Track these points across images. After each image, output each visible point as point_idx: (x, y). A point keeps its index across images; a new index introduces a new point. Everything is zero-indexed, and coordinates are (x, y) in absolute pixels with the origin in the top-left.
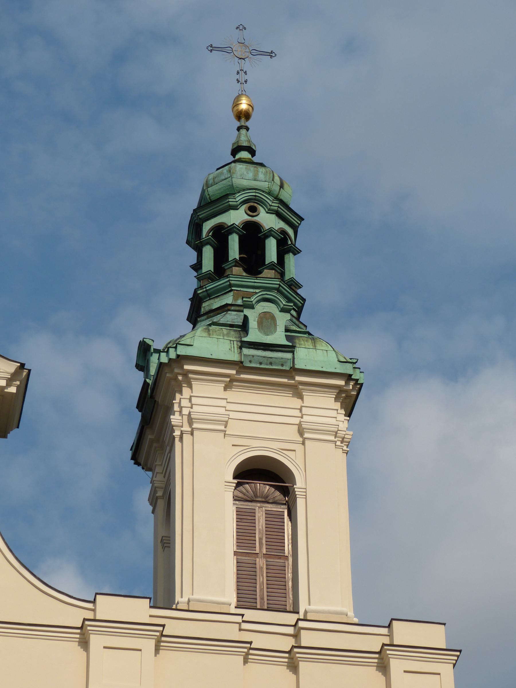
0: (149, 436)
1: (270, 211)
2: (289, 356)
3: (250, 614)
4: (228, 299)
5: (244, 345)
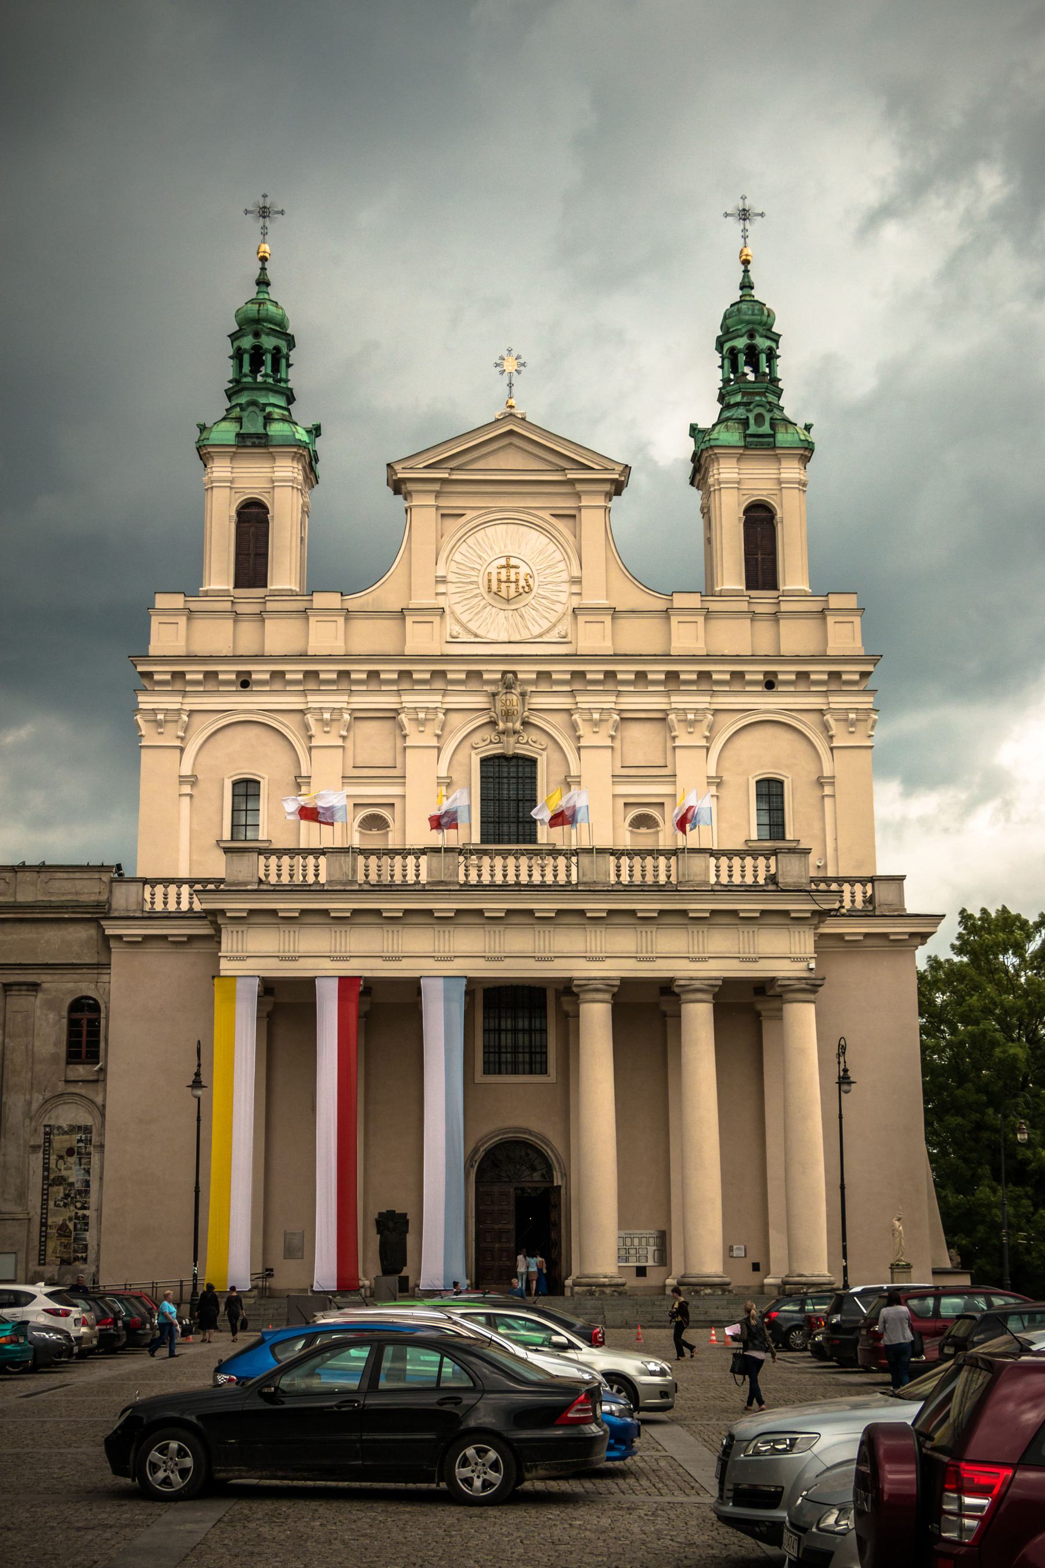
0: (698, 477)
1: (762, 336)
2: (772, 440)
3: (753, 593)
4: (738, 398)
5: (746, 436)
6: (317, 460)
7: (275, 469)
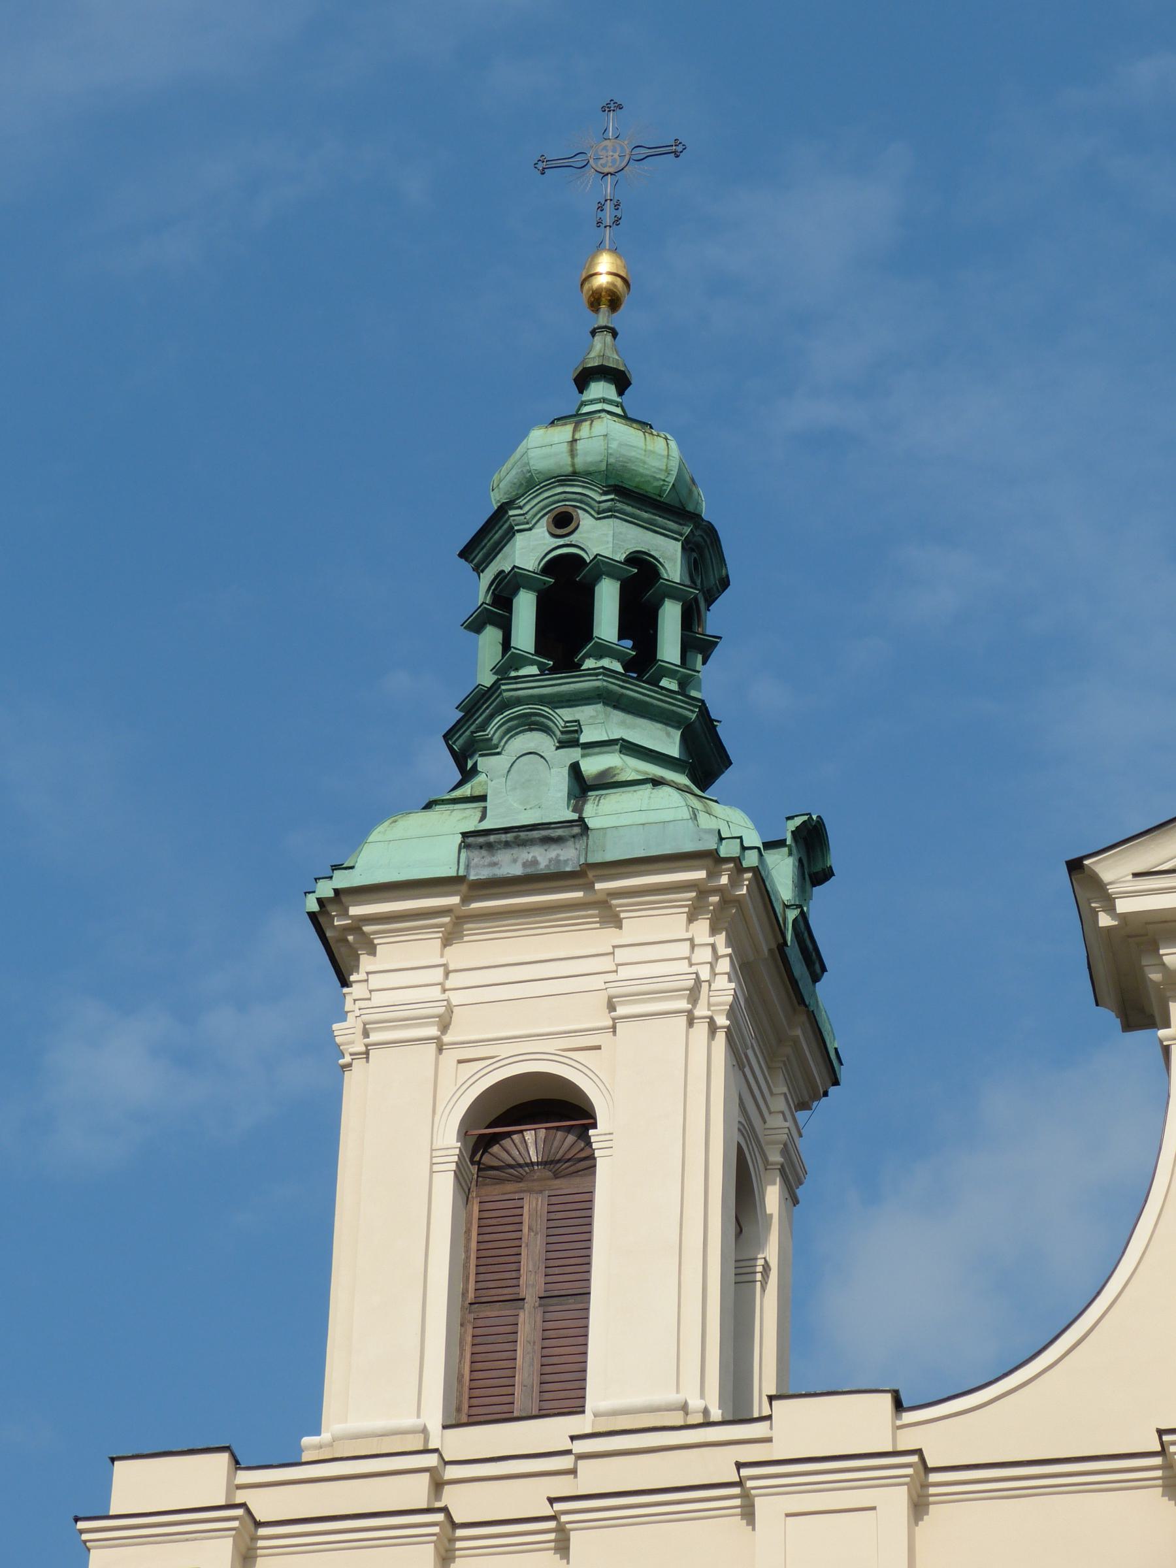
6: (815, 965)
7: (622, 955)
